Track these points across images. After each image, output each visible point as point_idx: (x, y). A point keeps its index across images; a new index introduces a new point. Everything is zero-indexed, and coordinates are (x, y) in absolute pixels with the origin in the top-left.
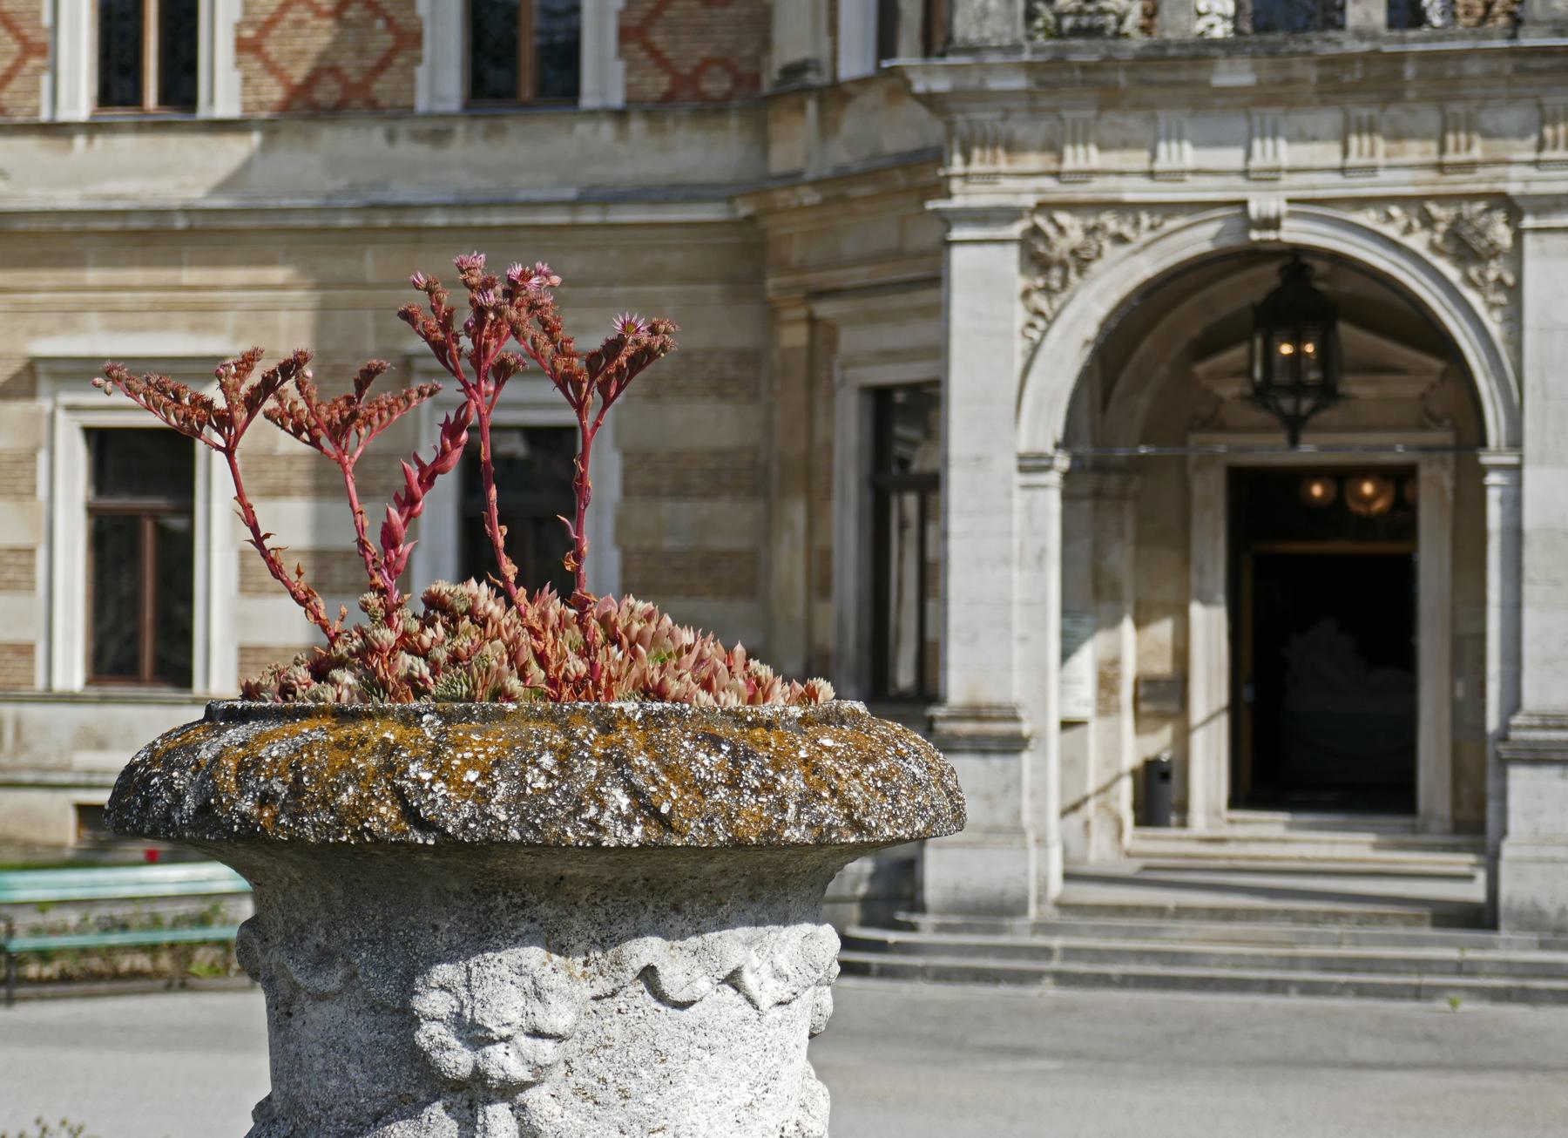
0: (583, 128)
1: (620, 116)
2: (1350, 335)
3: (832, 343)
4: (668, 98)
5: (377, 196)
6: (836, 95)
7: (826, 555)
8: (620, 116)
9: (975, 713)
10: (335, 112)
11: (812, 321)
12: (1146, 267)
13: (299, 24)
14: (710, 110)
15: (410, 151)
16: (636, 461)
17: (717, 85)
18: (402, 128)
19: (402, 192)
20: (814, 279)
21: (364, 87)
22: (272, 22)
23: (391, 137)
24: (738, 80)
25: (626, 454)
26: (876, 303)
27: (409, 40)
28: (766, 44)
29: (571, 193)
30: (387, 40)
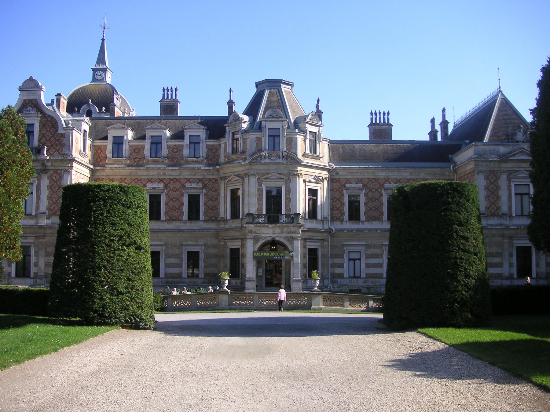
0: (200, 223)
1: (204, 221)
2: (278, 246)
3: (226, 244)
4: (209, 220)
5: (179, 228)
6: (227, 220)
7: (226, 264)
8: (204, 221)
9: (250, 278)
10: (175, 220)
11: (224, 241)
12: (263, 241)
13: (171, 211)
14: (213, 221)
15: (182, 224)
16: (205, 254)
17: (213, 218)
18: (182, 222)
19: (182, 228)
20: (225, 238)
21: (178, 218)
22: (168, 211)
23: (181, 223)
24: (215, 218)
25: (204, 254)
26: (232, 241)
27: (183, 213)
28: (219, 215)
29: (199, 229)
30: (181, 213)
